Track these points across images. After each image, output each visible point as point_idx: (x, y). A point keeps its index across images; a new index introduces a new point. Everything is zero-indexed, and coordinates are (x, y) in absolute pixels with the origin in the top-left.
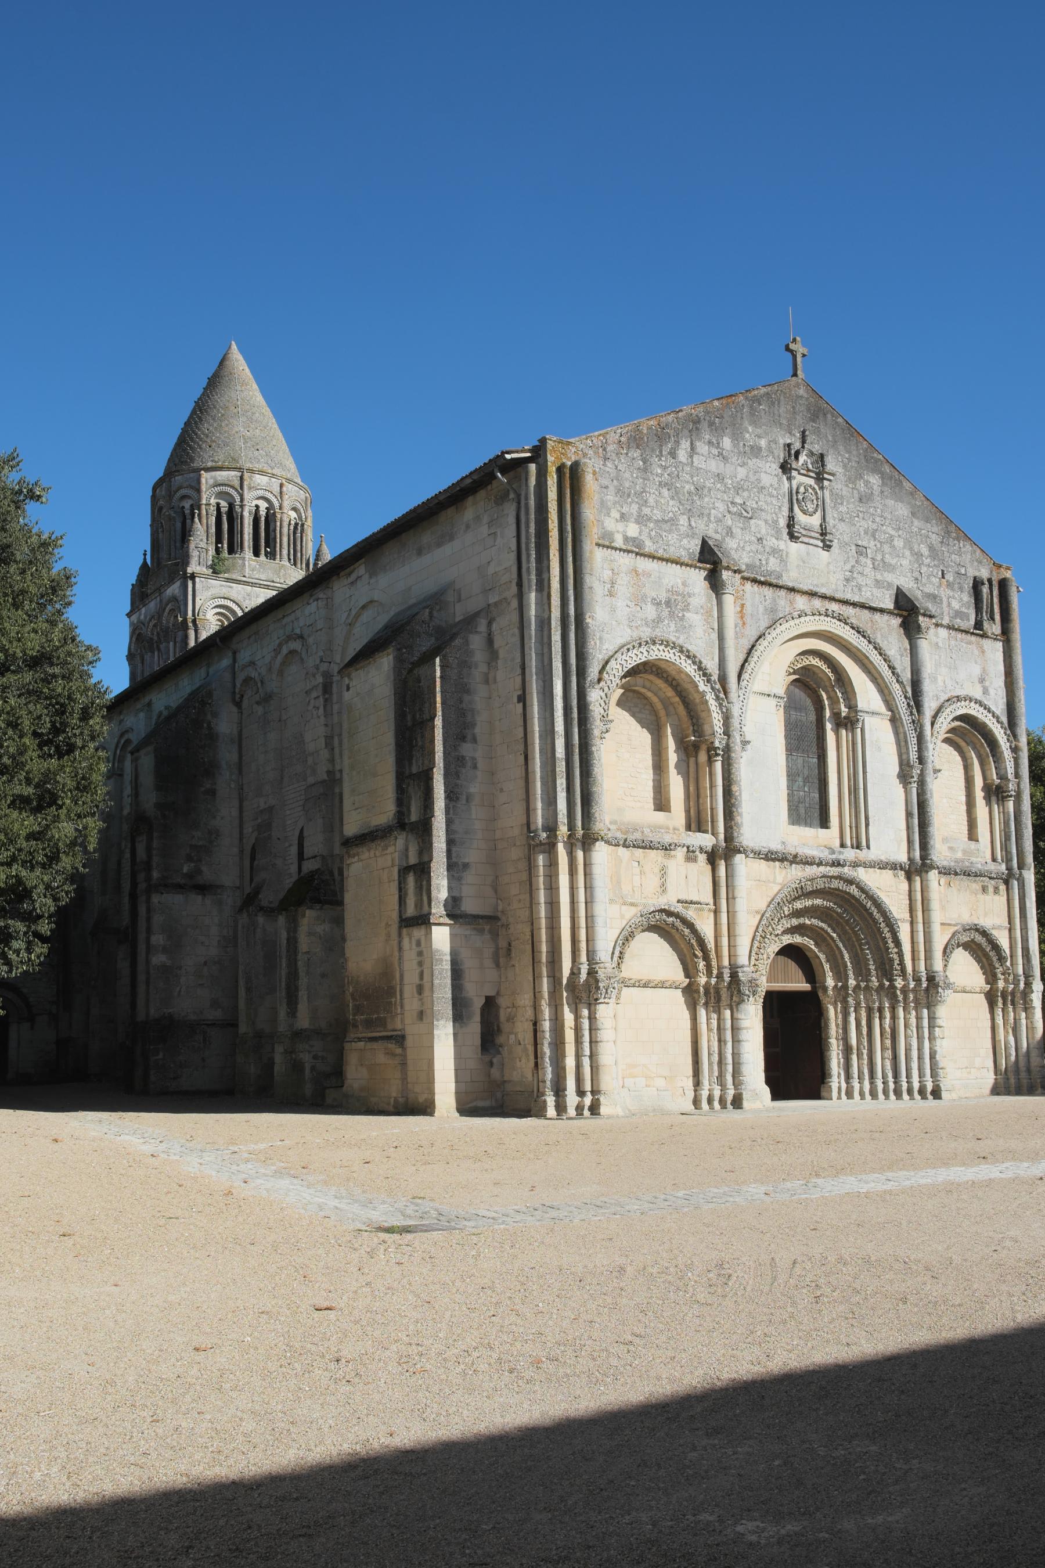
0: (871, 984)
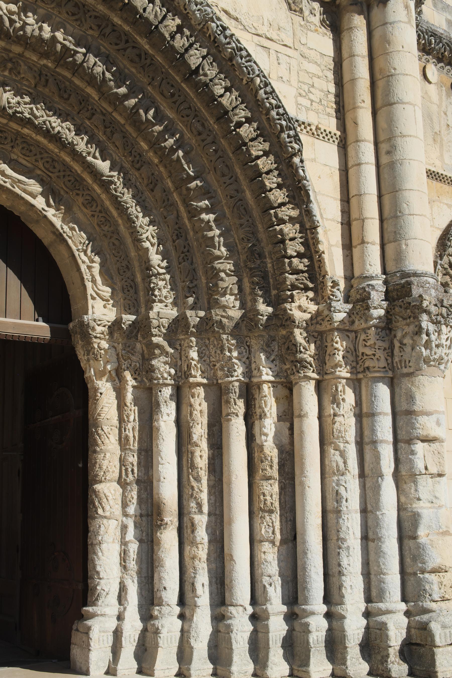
0: (217, 314)
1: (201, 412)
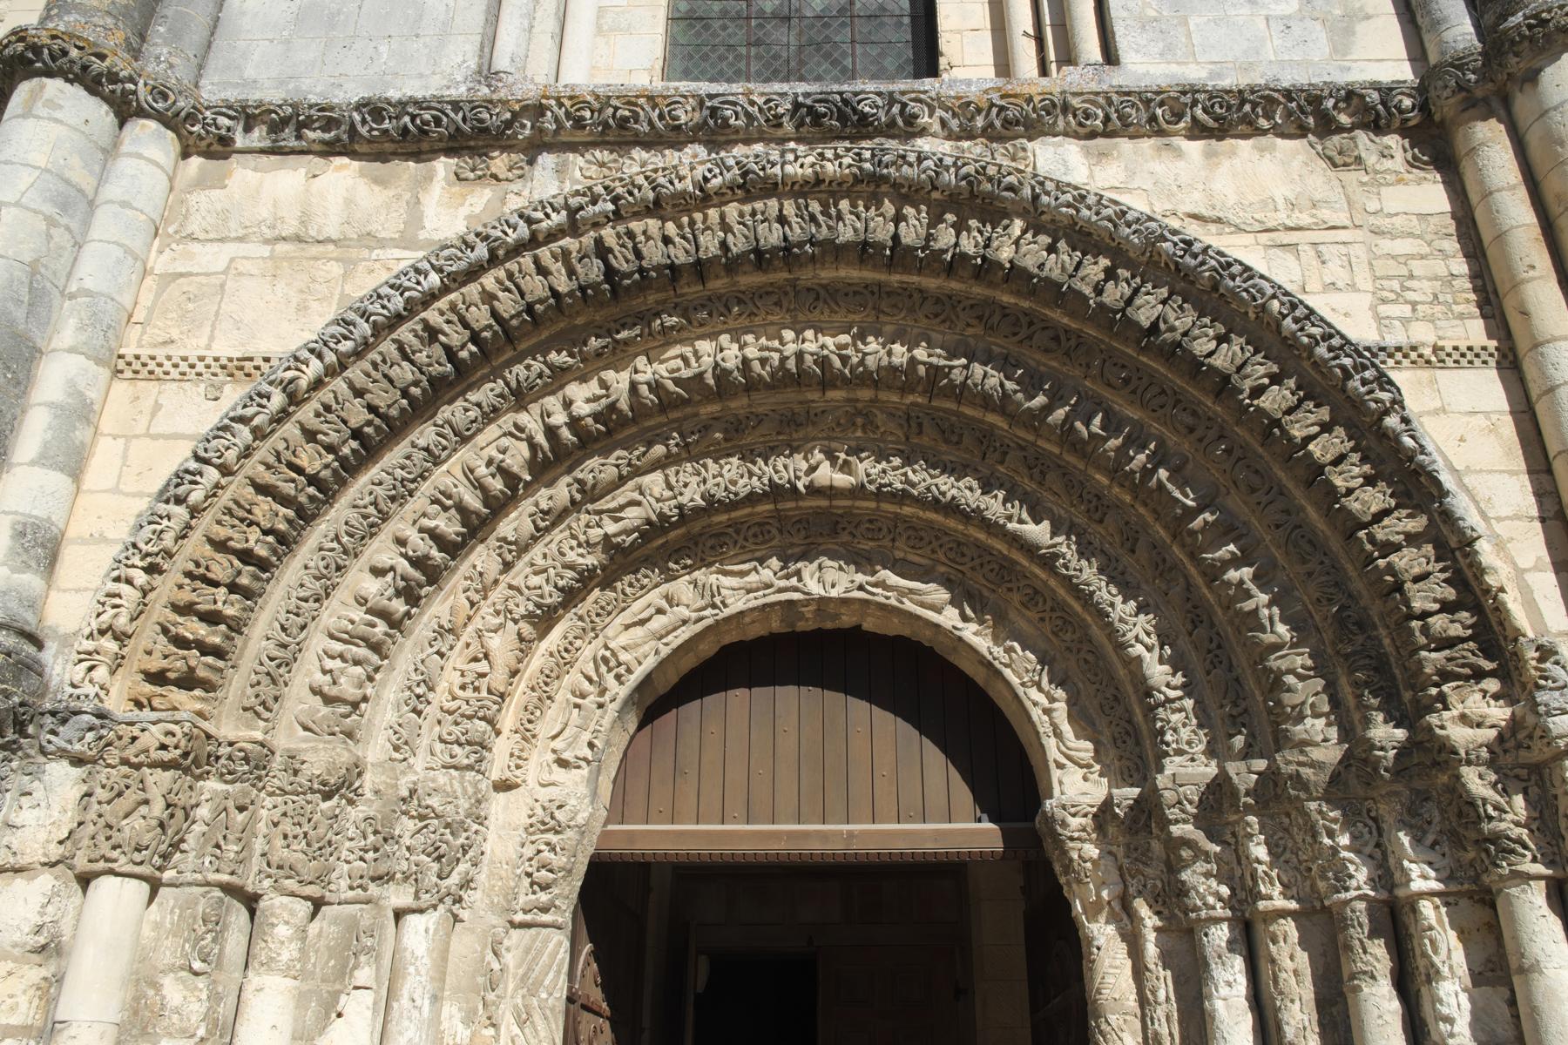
0: (1288, 761)
1: (1296, 973)
